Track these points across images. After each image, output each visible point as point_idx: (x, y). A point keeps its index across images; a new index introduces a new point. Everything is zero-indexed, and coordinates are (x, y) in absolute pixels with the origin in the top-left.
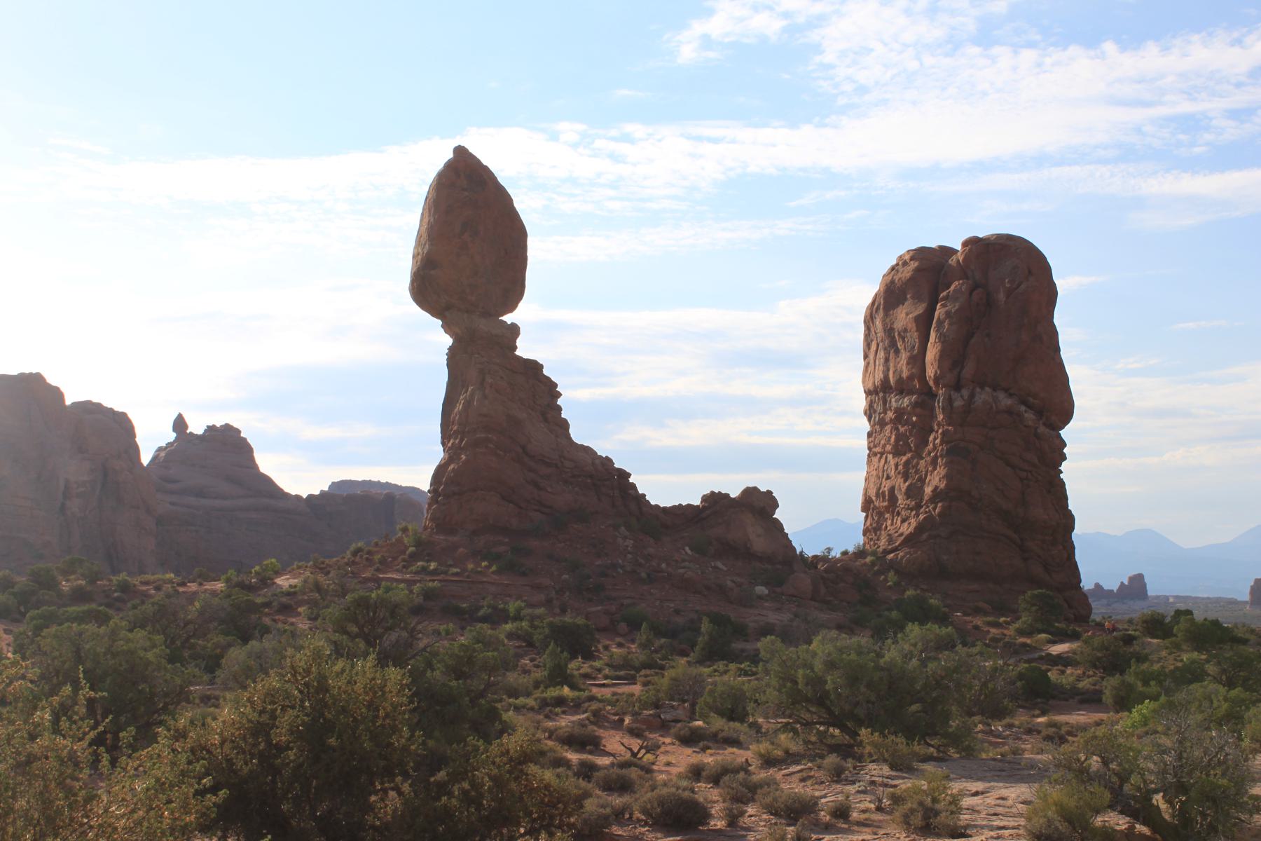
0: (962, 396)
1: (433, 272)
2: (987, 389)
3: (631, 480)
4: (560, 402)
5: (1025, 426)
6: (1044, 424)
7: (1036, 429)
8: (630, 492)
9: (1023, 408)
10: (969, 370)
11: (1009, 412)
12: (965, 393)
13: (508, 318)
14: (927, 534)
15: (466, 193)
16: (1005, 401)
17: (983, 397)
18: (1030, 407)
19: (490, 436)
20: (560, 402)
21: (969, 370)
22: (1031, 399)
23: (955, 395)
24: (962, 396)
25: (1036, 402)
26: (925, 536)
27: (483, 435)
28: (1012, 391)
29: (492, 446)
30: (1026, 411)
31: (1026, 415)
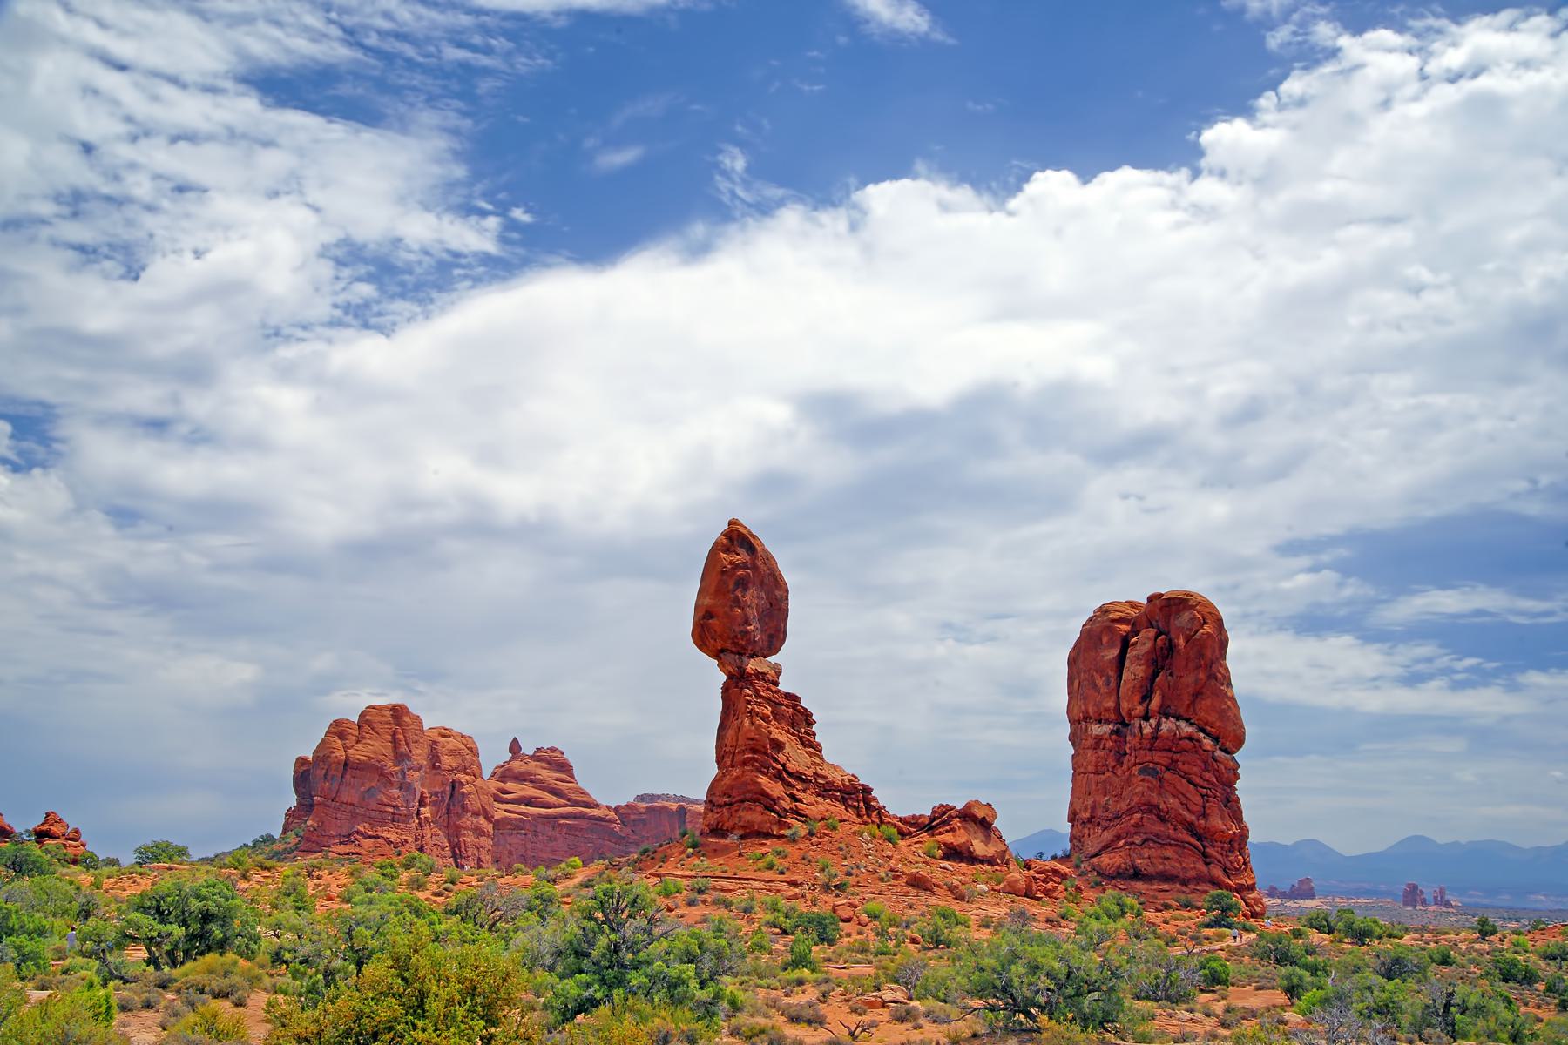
0: (1150, 725)
1: (710, 621)
2: (1172, 719)
4: (814, 728)
5: (1205, 751)
6: (1220, 749)
9: (1202, 735)
10: (1155, 702)
11: (1190, 738)
12: (1153, 722)
13: (772, 659)
14: (1123, 841)
15: (738, 557)
16: (1187, 729)
17: (1167, 725)
20: (814, 728)
21: (1155, 702)
22: (1209, 728)
23: (1144, 724)
24: (1150, 725)
27: (750, 755)
28: (1192, 721)
30: (1204, 738)
31: (1205, 741)
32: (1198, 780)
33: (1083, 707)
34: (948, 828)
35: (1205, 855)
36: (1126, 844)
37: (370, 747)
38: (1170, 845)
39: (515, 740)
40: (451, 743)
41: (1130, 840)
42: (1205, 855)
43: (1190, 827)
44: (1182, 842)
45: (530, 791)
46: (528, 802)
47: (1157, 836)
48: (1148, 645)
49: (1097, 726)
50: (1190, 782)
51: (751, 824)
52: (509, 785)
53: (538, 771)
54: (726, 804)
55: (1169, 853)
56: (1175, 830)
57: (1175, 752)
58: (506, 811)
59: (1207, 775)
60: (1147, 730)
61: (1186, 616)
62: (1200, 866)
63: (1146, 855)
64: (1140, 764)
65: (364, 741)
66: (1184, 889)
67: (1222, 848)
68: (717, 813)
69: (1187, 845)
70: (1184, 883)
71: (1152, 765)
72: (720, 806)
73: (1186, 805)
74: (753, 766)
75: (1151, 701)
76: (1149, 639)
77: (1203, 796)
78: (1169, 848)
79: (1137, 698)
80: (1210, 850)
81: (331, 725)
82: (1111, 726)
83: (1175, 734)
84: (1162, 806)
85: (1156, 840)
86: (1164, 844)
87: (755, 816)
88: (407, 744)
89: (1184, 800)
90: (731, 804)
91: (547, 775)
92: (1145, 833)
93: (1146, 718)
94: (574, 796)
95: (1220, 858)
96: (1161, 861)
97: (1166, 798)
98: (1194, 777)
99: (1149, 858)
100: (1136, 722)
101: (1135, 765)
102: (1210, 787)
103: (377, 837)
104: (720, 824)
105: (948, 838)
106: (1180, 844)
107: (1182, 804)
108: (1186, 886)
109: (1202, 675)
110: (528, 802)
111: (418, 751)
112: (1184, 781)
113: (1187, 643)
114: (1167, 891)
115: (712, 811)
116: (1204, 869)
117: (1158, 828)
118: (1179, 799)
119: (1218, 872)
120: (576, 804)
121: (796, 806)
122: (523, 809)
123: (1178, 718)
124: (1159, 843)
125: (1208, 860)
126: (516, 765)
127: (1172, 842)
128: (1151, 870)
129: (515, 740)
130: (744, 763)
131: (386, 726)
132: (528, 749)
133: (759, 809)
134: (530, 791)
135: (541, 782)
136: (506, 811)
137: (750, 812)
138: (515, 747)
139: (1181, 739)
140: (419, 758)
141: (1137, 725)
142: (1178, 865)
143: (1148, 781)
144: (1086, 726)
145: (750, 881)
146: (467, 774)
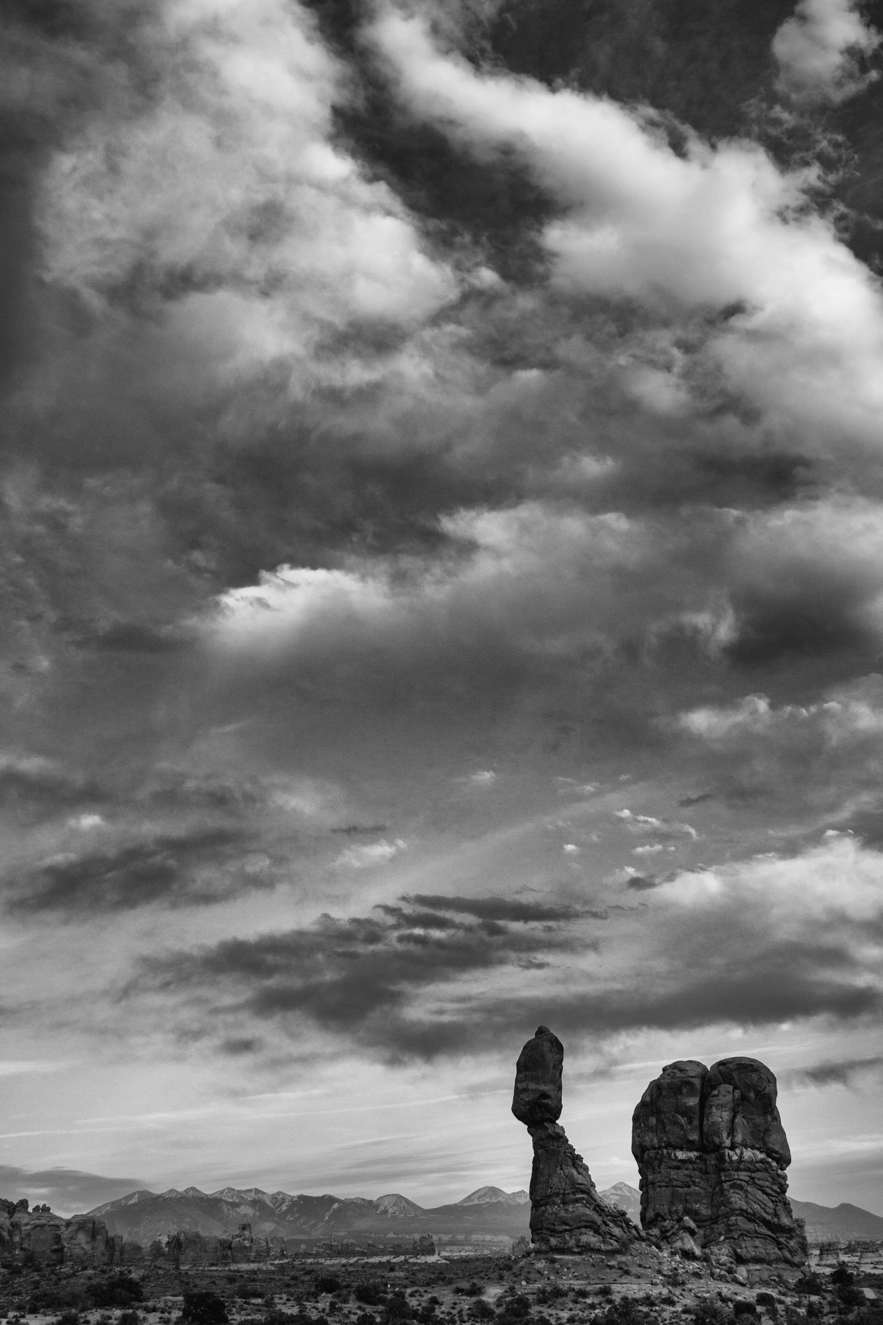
0: (736, 1154)
1: (544, 1101)
2: (750, 1149)
3: (627, 1216)
7: (777, 1171)
8: (630, 1223)
9: (770, 1160)
11: (762, 1161)
12: (738, 1151)
16: (761, 1156)
17: (748, 1154)
18: (774, 1159)
19: (584, 1196)
21: (739, 1138)
23: (731, 1153)
24: (736, 1154)
25: (777, 1156)
26: (722, 1238)
28: (762, 1150)
29: (585, 1202)
32: (769, 1191)
33: (665, 1139)
34: (678, 1238)
35: (778, 1243)
36: (726, 1238)
38: (757, 1237)
41: (728, 1236)
42: (778, 1243)
43: (767, 1224)
44: (764, 1235)
47: (748, 1231)
48: (729, 1097)
49: (681, 1153)
50: (764, 1193)
51: (588, 1244)
54: (566, 1230)
55: (757, 1242)
56: (759, 1227)
57: (752, 1172)
59: (775, 1188)
60: (735, 1158)
61: (754, 1076)
62: (776, 1250)
63: (744, 1246)
64: (729, 1181)
66: (769, 1267)
67: (787, 1238)
68: (558, 1237)
69: (767, 1237)
70: (769, 1263)
71: (739, 1182)
72: (561, 1232)
73: (764, 1209)
74: (582, 1203)
75: (733, 1136)
76: (729, 1092)
77: (773, 1202)
78: (756, 1239)
79: (725, 1135)
80: (782, 1240)
82: (696, 1153)
83: (753, 1160)
84: (750, 1211)
85: (748, 1234)
86: (754, 1237)
87: (589, 1238)
89: (762, 1205)
90: (570, 1231)
92: (740, 1230)
93: (733, 1147)
95: (786, 1243)
96: (753, 1249)
97: (752, 1205)
98: (767, 1189)
99: (746, 1248)
100: (727, 1151)
101: (726, 1181)
102: (777, 1195)
104: (562, 1245)
105: (678, 1244)
106: (764, 1237)
107: (761, 1208)
108: (771, 1265)
109: (769, 1119)
112: (760, 1192)
113: (756, 1095)
114: (759, 1270)
115: (551, 1236)
116: (780, 1253)
117: (750, 1226)
118: (759, 1205)
119: (788, 1255)
121: (609, 1230)
123: (753, 1148)
124: (750, 1237)
125: (780, 1246)
127: (759, 1235)
128: (748, 1256)
130: (577, 1201)
133: (591, 1233)
137: (585, 1236)
139: (757, 1162)
141: (727, 1154)
142: (764, 1252)
143: (738, 1194)
144: (668, 1153)
145: (630, 1285)
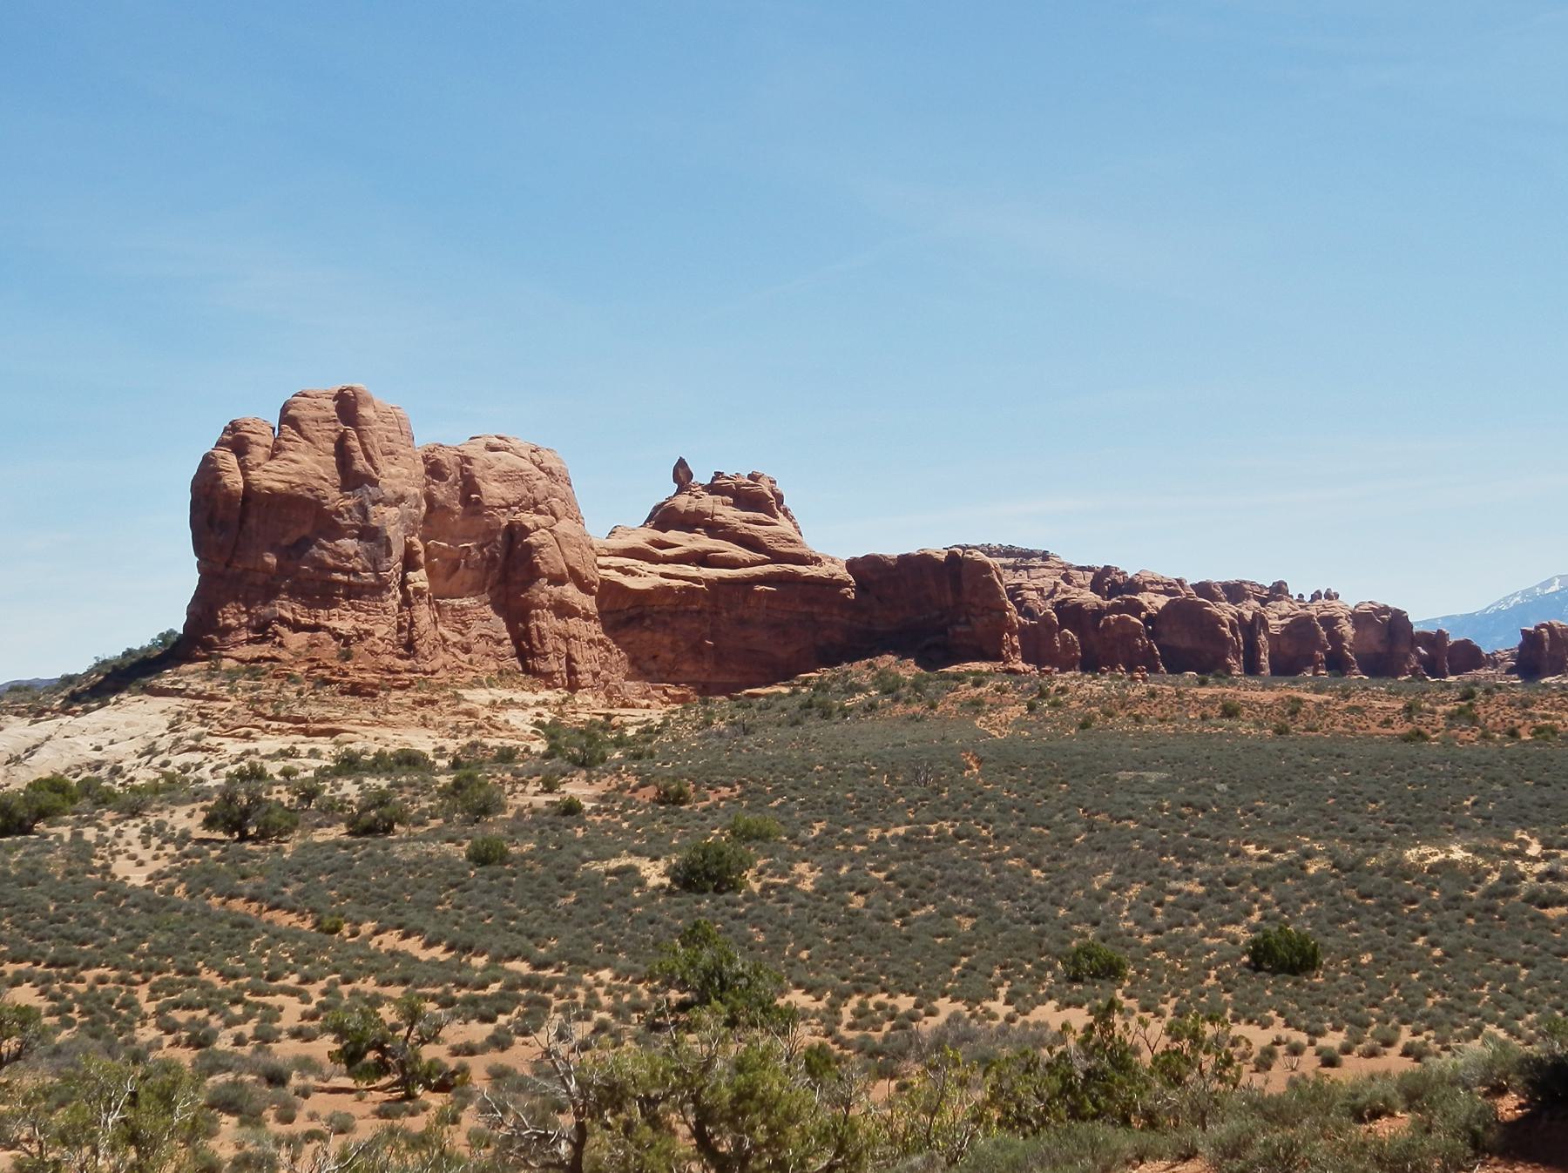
37: (293, 465)
39: (681, 464)
40: (505, 461)
45: (702, 542)
46: (702, 559)
52: (671, 536)
53: (719, 509)
58: (663, 575)
65: (281, 456)
81: (226, 429)
88: (369, 458)
91: (729, 514)
94: (777, 547)
103: (316, 628)
110: (702, 559)
111: (393, 470)
120: (778, 558)
122: (691, 570)
126: (683, 502)
129: (681, 464)
131: (327, 426)
132: (702, 476)
134: (702, 542)
135: (723, 525)
136: (663, 575)
138: (682, 474)
140: (396, 482)
146: (539, 512)
